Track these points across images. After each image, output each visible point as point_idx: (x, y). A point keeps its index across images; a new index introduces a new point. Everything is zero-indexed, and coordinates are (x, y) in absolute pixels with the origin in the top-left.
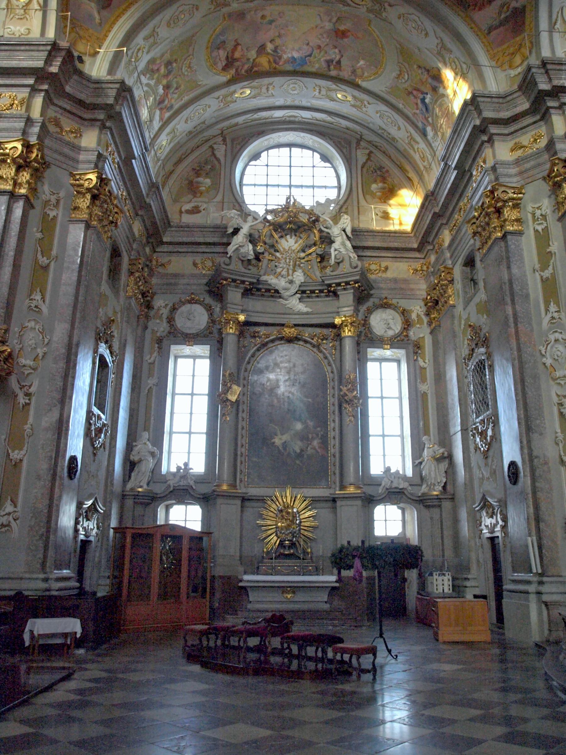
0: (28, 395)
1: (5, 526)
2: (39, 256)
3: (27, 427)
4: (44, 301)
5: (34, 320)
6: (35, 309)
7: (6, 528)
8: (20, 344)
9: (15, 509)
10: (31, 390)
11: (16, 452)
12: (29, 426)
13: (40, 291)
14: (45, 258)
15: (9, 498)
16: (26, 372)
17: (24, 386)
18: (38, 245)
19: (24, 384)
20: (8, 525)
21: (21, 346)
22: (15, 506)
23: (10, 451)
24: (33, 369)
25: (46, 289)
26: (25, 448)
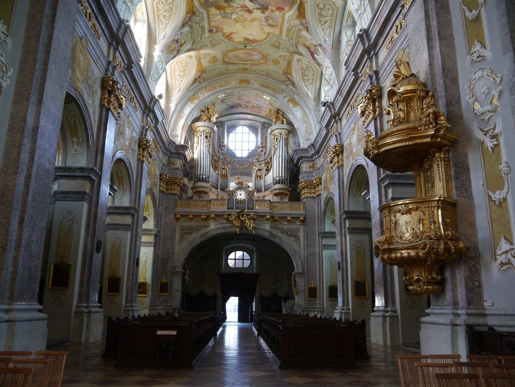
0: (494, 137)
1: (506, 264)
2: (468, 13)
3: (503, 167)
4: (485, 48)
5: (480, 69)
6: (479, 59)
7: (507, 266)
8: (473, 96)
9: (512, 247)
10: (496, 131)
11: (498, 192)
12: (504, 164)
13: (478, 42)
14: (474, 11)
15: (503, 237)
16: (486, 118)
17: (487, 131)
18: (463, 6)
19: (488, 129)
20: (509, 263)
21: (474, 98)
22: (511, 244)
23: (491, 194)
24: (492, 112)
25: (483, 36)
26: (506, 186)
